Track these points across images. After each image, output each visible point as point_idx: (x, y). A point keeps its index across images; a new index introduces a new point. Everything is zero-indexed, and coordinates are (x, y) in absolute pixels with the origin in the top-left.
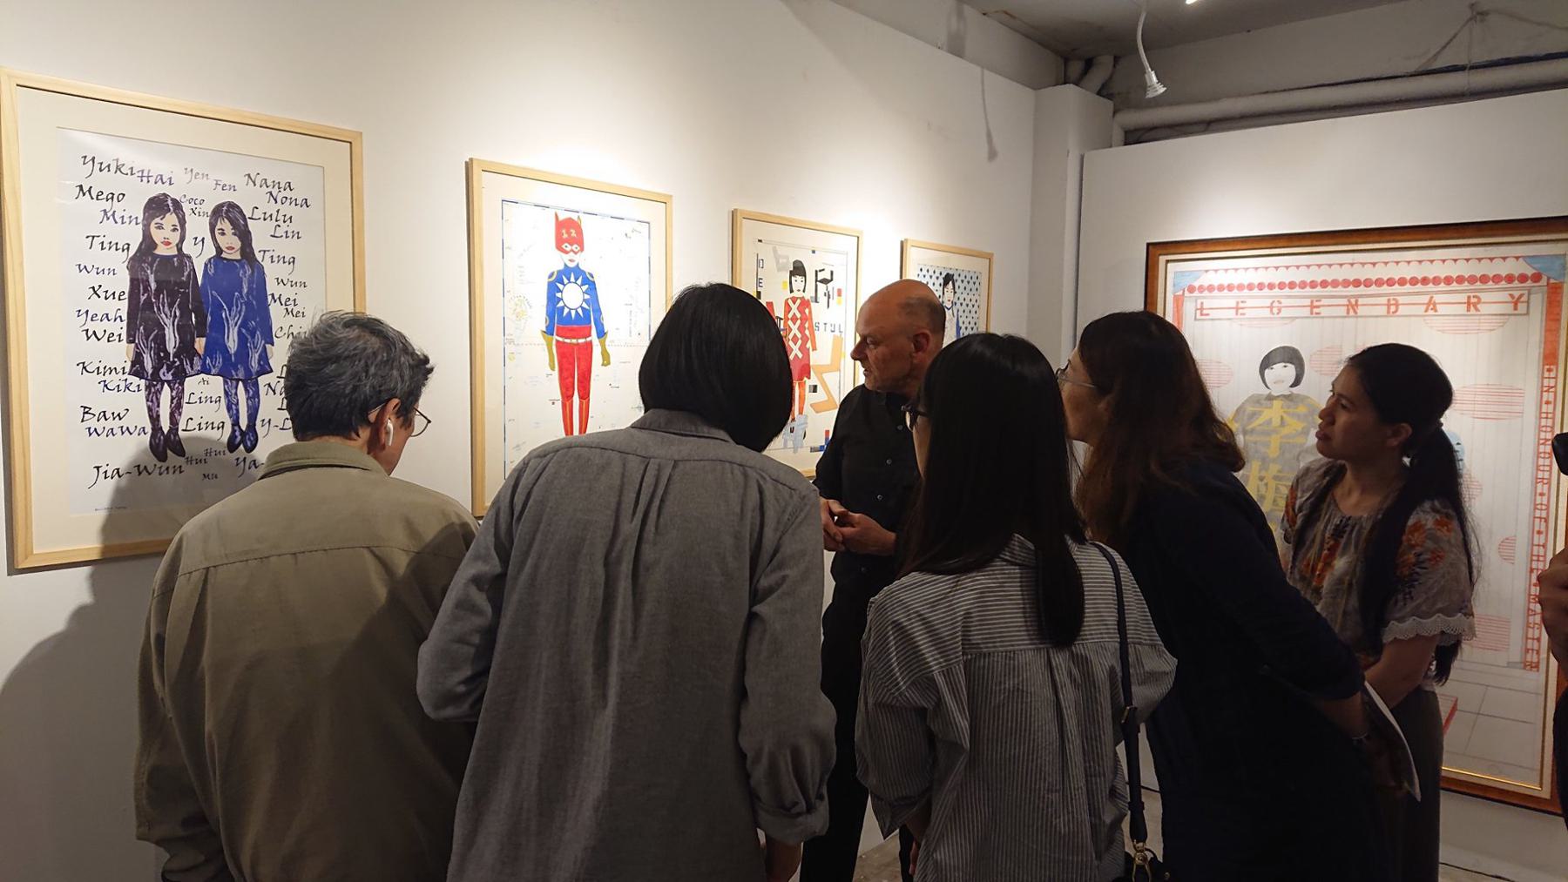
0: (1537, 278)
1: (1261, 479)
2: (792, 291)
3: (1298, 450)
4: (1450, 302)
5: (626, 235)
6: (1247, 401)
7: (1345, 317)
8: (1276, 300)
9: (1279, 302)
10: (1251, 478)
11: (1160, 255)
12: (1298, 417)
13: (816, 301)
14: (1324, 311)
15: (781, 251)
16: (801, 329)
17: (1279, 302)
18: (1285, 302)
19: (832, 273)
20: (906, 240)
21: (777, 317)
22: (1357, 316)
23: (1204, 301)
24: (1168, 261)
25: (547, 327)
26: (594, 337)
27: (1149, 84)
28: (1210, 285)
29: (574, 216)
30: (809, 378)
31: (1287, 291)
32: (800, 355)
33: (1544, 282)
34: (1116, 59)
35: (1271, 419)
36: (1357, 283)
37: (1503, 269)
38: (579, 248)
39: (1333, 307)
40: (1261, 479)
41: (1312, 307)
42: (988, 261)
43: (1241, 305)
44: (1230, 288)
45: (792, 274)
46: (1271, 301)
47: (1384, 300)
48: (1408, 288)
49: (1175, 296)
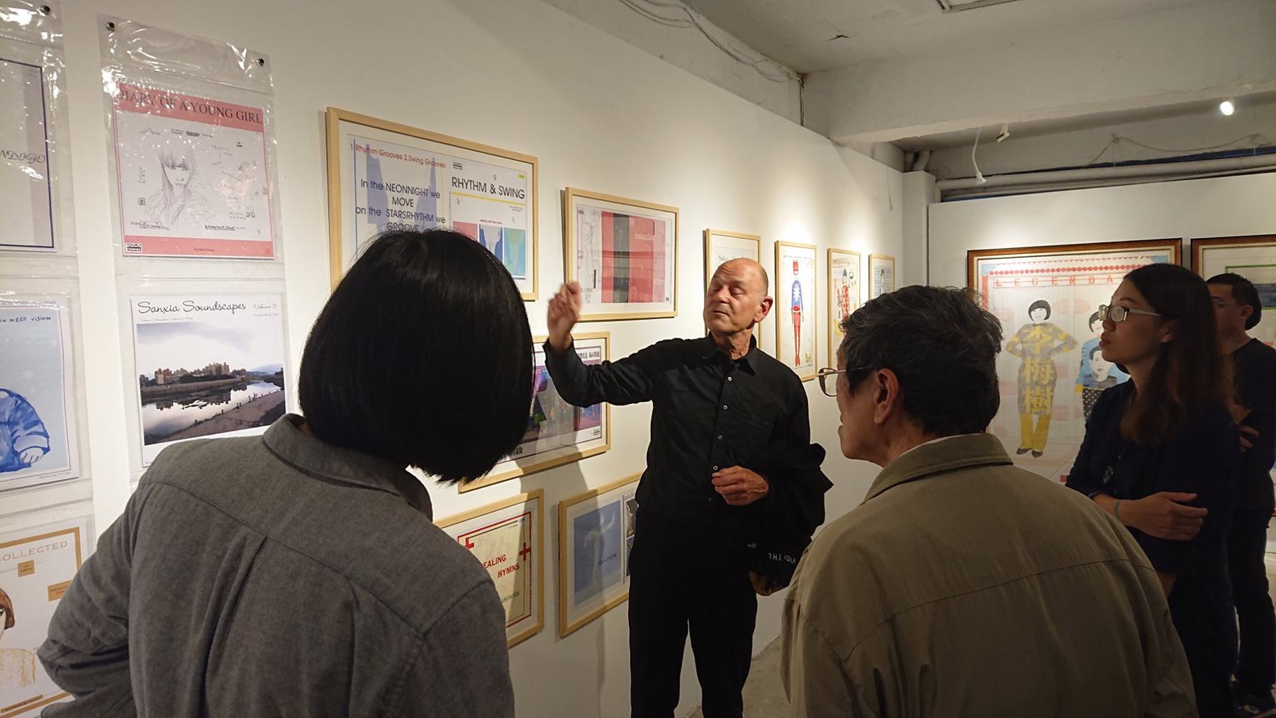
1: (1032, 365)
6: (1023, 327)
7: (1068, 285)
10: (1026, 366)
14: (1059, 283)
16: (846, 301)
26: (801, 311)
31: (1040, 273)
34: (931, 152)
36: (1074, 269)
39: (1063, 279)
40: (1032, 365)
41: (1053, 281)
44: (1011, 272)
47: (1087, 277)
48: (1098, 271)
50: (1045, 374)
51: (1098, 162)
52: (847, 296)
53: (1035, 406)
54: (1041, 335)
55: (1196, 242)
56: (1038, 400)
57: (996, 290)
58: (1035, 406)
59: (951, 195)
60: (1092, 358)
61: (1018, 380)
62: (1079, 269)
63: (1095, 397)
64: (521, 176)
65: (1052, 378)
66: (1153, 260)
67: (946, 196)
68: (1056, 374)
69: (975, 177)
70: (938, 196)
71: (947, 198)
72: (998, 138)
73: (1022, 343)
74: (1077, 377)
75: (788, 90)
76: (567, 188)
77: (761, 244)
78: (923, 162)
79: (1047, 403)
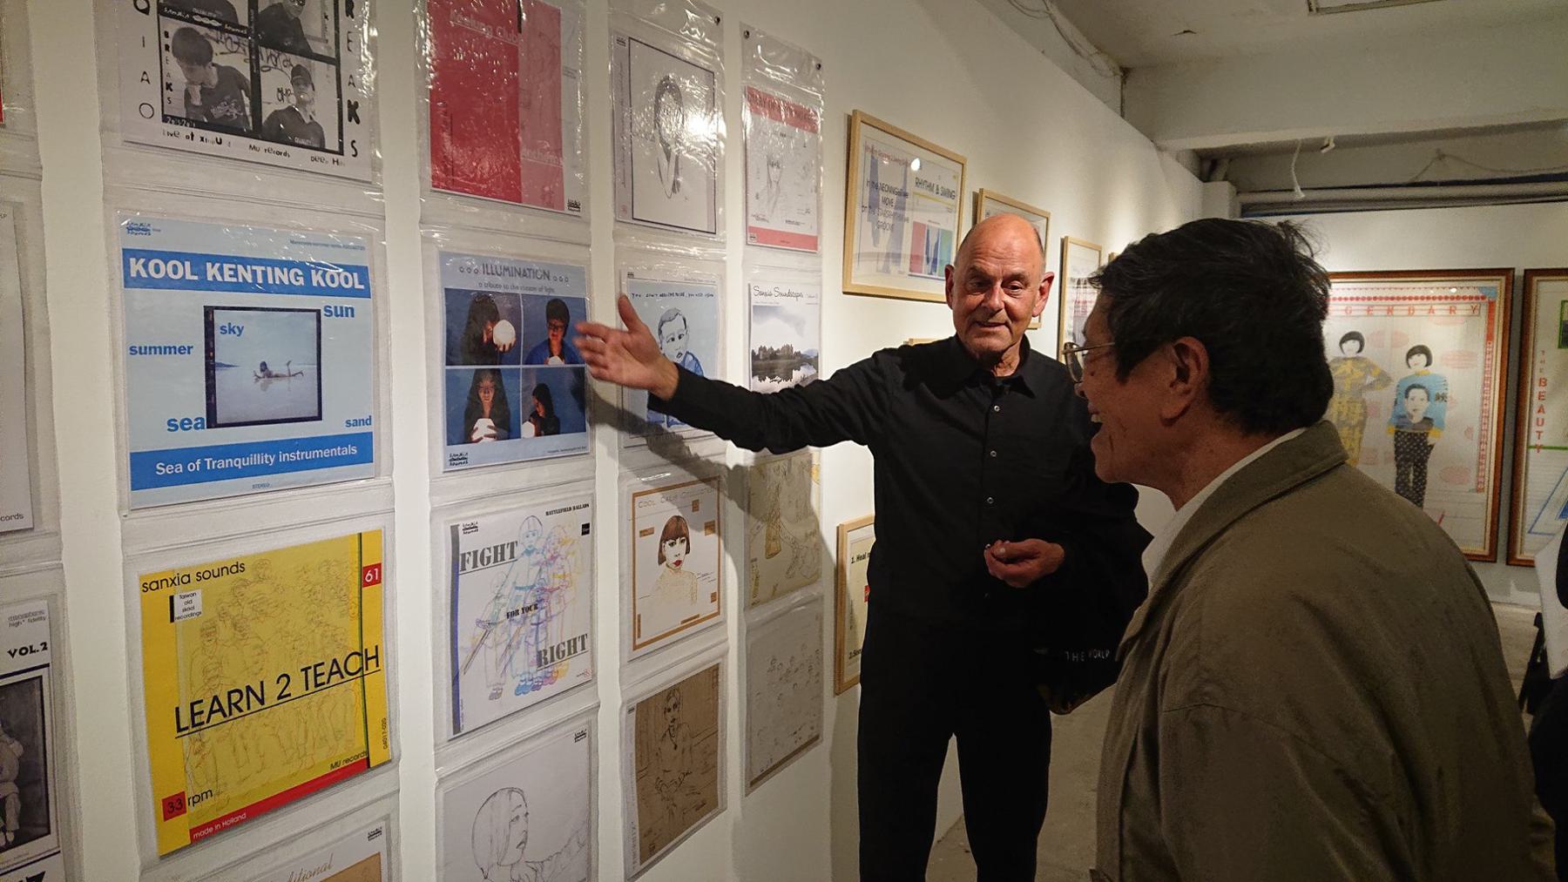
0: (1483, 298)
4: (1441, 309)
7: (1385, 316)
14: (1375, 313)
18: (1353, 308)
22: (1393, 315)
31: (1354, 302)
33: (1487, 300)
34: (1231, 160)
36: (1392, 299)
37: (1468, 293)
39: (1379, 311)
40: (1340, 403)
41: (1369, 311)
47: (1407, 308)
48: (1419, 301)
51: (1420, 180)
54: (1352, 371)
55: (1530, 273)
59: (1252, 211)
60: (1407, 397)
62: (1398, 298)
63: (1409, 440)
64: (954, 177)
65: (1362, 418)
66: (1481, 291)
69: (1292, 190)
71: (1246, 213)
72: (1322, 148)
74: (1390, 417)
75: (1112, 84)
76: (981, 190)
77: (1102, 253)
78: (1220, 173)
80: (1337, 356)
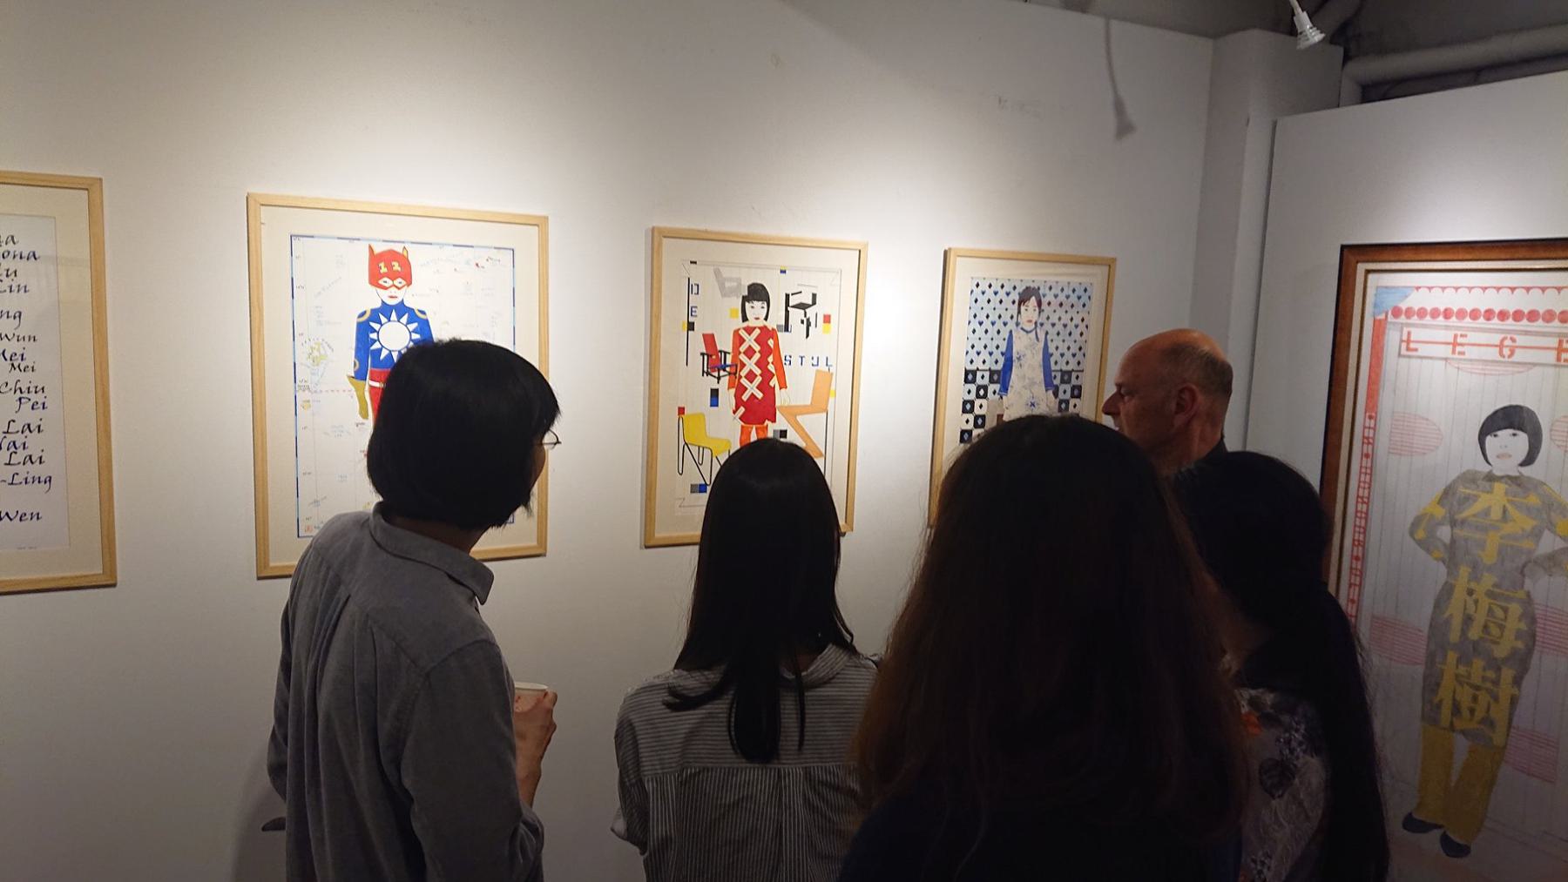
1: (1470, 592)
2: (745, 319)
3: (1524, 558)
5: (477, 265)
6: (1458, 477)
8: (1509, 336)
9: (1513, 340)
10: (1456, 590)
11: (1357, 262)
12: (1528, 510)
13: (787, 329)
15: (726, 272)
16: (761, 364)
17: (1513, 340)
19: (814, 296)
20: (950, 249)
21: (721, 352)
23: (1413, 330)
24: (1368, 272)
25: (355, 372)
27: (1299, 31)
28: (1422, 308)
29: (398, 248)
30: (774, 421)
32: (760, 395)
35: (1490, 507)
38: (404, 282)
40: (1470, 592)
42: (1108, 268)
43: (1460, 340)
44: (1447, 314)
45: (745, 299)
46: (1503, 336)
49: (1374, 321)
50: (1502, 627)
52: (766, 350)
53: (1466, 713)
54: (1505, 511)
56: (1475, 699)
57: (1403, 361)
58: (1466, 713)
61: (1431, 625)
65: (1520, 645)
67: (1374, 91)
68: (1533, 636)
70: (1348, 88)
73: (1453, 523)
79: (1499, 713)
80: (1470, 467)
